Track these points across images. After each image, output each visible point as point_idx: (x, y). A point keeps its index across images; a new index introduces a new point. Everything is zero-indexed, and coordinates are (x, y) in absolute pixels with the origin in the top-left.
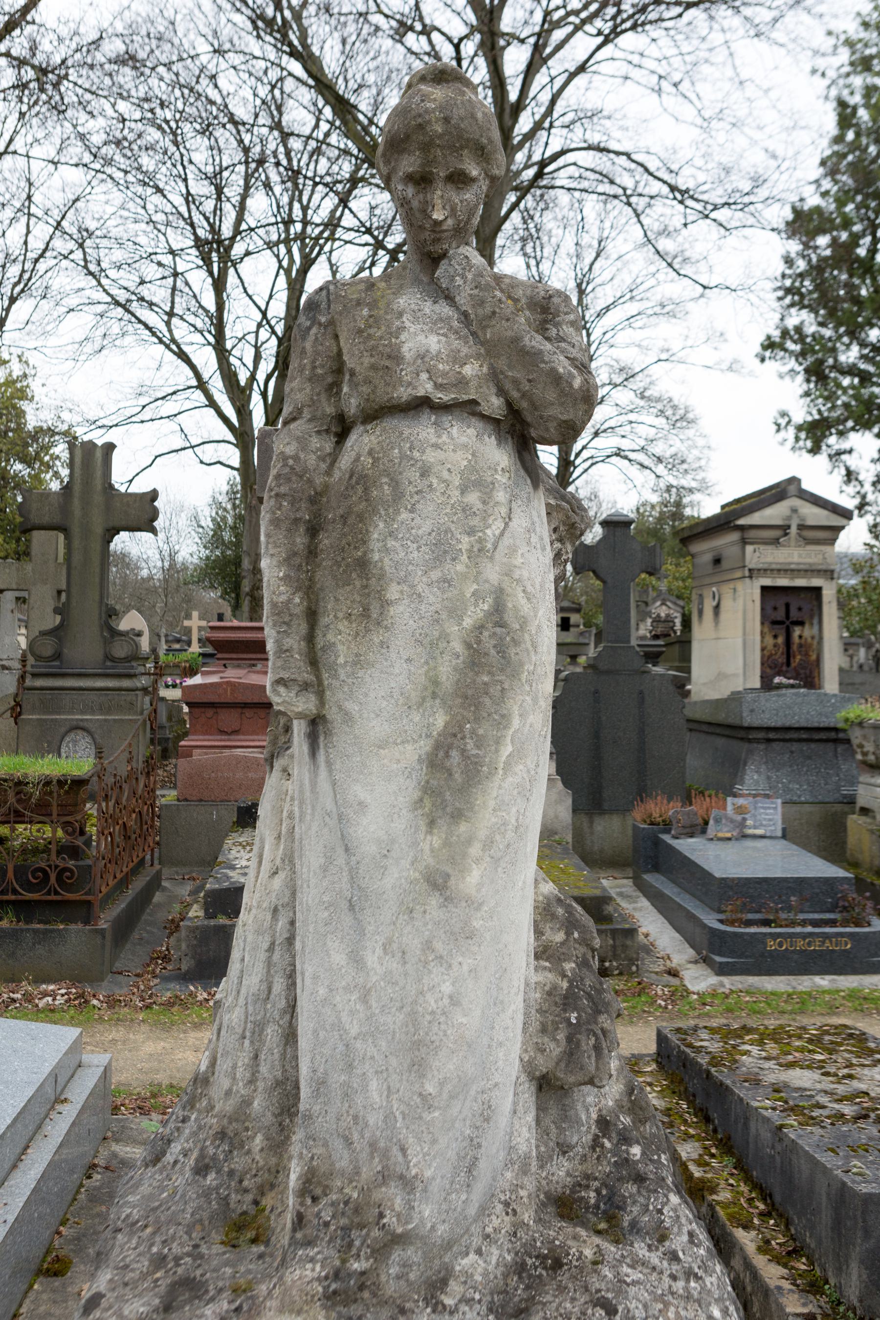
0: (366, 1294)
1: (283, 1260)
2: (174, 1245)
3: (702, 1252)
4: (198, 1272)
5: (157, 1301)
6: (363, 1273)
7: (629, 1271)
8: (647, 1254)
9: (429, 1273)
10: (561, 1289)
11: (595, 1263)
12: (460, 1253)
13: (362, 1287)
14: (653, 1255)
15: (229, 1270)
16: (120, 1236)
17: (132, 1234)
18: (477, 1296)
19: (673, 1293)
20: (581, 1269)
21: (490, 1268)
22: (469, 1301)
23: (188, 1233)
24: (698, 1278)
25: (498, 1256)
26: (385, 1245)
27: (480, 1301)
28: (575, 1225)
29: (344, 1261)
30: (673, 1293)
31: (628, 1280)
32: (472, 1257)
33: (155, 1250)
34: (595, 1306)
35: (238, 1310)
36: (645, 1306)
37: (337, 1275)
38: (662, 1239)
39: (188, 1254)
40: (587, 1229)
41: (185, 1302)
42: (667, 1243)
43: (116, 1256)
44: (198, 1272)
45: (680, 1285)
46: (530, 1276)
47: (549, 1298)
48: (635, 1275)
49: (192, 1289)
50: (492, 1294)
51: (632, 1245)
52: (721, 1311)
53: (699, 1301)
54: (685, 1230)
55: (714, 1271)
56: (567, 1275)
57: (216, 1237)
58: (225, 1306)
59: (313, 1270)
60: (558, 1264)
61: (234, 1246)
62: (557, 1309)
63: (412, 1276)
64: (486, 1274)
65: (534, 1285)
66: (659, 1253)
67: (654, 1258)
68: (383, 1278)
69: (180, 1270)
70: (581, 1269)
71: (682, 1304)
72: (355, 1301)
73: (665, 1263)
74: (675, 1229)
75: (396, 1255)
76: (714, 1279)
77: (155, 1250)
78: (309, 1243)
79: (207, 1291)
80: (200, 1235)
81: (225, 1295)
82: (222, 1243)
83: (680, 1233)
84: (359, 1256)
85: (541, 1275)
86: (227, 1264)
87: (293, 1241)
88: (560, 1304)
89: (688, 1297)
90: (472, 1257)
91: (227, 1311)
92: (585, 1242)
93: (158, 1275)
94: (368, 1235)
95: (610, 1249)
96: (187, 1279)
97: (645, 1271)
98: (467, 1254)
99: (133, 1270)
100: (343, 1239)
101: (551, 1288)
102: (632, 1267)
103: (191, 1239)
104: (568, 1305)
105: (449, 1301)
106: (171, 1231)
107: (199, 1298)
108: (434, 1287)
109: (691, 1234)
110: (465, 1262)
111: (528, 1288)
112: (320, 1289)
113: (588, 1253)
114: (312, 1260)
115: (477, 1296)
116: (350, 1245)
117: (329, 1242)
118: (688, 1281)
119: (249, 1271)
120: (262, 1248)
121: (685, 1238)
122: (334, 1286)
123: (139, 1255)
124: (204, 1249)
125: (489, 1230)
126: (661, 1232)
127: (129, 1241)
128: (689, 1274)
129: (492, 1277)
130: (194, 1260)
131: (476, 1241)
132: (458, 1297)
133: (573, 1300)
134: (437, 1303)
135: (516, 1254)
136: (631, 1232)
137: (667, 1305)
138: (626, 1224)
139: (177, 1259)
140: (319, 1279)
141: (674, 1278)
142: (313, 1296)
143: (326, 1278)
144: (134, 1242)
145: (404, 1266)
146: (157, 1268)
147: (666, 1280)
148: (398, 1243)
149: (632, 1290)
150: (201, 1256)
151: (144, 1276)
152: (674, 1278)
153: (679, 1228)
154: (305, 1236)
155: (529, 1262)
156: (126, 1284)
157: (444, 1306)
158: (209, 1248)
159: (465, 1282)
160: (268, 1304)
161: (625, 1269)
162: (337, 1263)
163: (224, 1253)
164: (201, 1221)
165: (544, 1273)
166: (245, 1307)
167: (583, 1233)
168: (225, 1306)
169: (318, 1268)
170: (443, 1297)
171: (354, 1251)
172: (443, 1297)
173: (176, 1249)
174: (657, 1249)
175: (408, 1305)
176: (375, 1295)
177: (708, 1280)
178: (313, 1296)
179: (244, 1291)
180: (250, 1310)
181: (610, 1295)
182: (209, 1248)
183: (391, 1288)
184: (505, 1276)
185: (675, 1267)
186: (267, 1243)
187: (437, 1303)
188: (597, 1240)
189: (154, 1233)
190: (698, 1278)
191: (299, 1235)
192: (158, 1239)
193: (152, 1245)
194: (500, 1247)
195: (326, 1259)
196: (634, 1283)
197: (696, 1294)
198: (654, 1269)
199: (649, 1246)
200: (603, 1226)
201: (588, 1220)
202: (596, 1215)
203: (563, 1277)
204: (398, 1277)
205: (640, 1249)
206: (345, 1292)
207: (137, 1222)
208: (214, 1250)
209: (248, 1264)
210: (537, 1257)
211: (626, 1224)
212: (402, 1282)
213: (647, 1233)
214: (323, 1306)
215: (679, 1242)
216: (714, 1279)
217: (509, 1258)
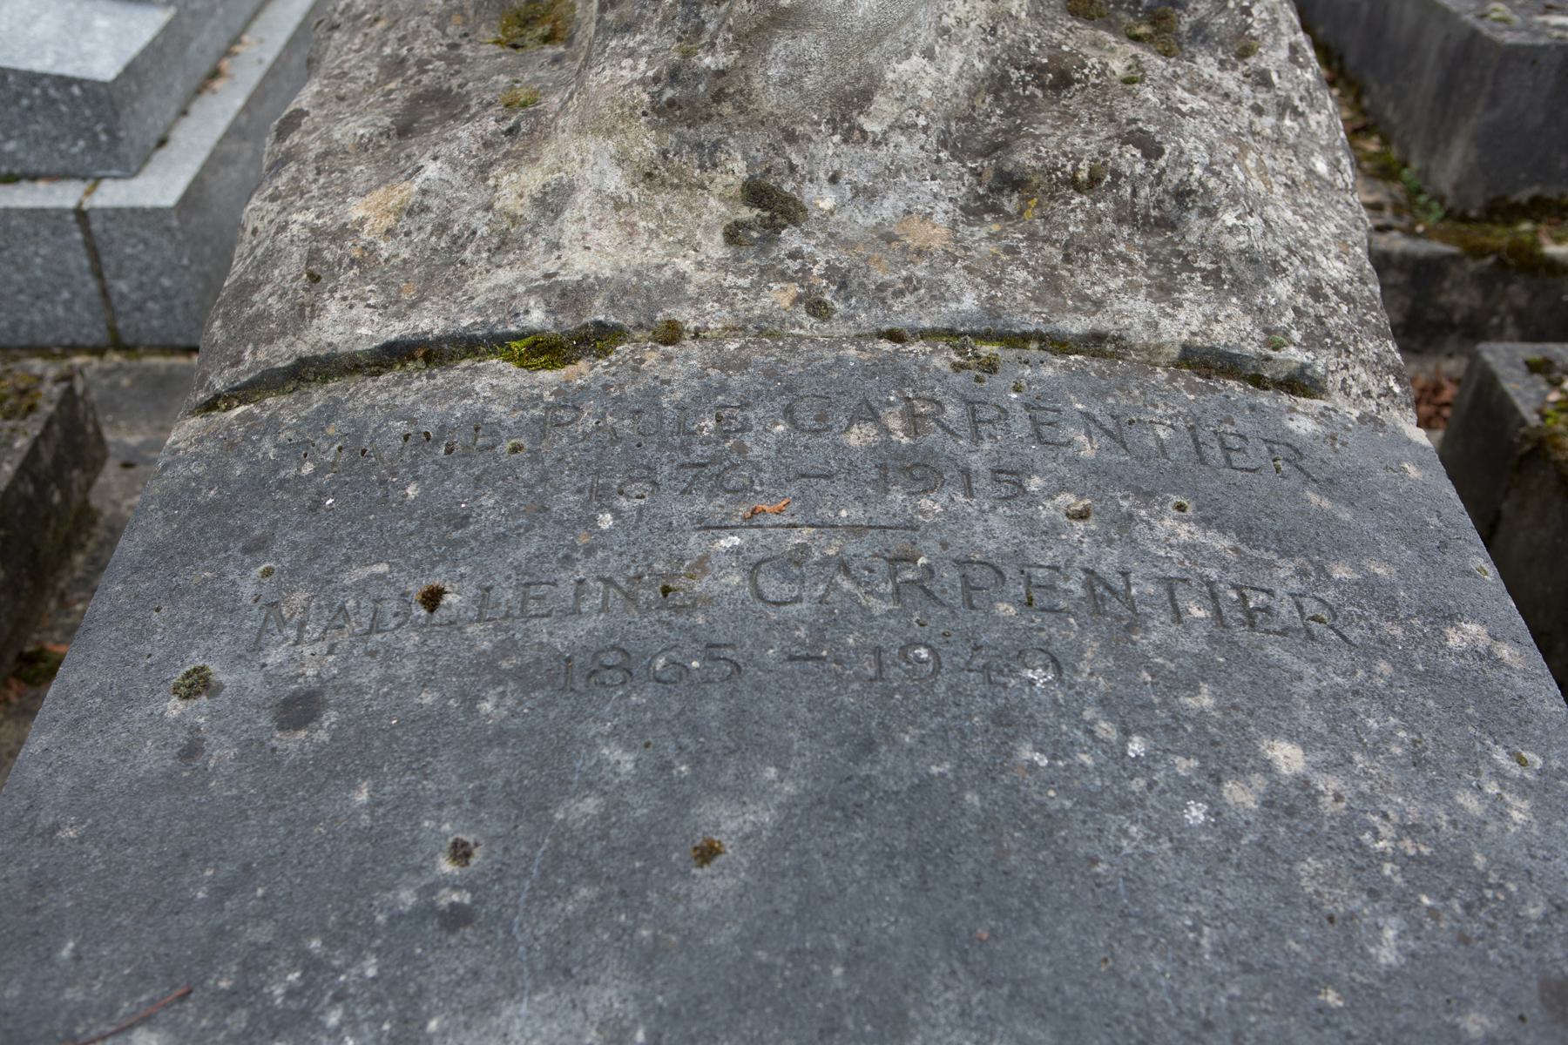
0: (727, 108)
1: (587, 59)
2: (417, 44)
3: (1309, 76)
4: (455, 82)
5: (387, 121)
6: (720, 73)
7: (1186, 95)
8: (1217, 74)
9: (840, 79)
10: (1067, 117)
11: (1128, 81)
12: (896, 53)
13: (719, 96)
14: (1226, 75)
15: (504, 79)
16: (337, 35)
17: (354, 30)
18: (922, 121)
19: (1254, 134)
20: (1103, 90)
21: (947, 80)
22: (907, 128)
23: (441, 27)
24: (1297, 114)
25: (959, 64)
26: (760, 27)
27: (925, 129)
28: (1097, 27)
29: (687, 55)
30: (1254, 134)
31: (1184, 108)
32: (917, 60)
33: (387, 51)
34: (1125, 143)
35: (510, 132)
36: (1211, 148)
37: (674, 76)
38: (1245, 53)
39: (440, 57)
40: (1115, 33)
41: (434, 123)
42: (1252, 60)
43: (329, 62)
44: (455, 82)
45: (1266, 123)
46: (1014, 97)
47: (1044, 129)
48: (1195, 103)
49: (445, 106)
50: (947, 120)
51: (1192, 59)
52: (1329, 164)
53: (1295, 148)
54: (1285, 41)
55: (1325, 107)
56: (1078, 98)
57: (487, 33)
58: (492, 125)
59: (634, 69)
60: (1063, 81)
61: (515, 47)
62: (1058, 146)
63: (809, 83)
64: (938, 88)
65: (1020, 111)
66: (1237, 74)
67: (1229, 81)
68: (757, 83)
69: (425, 79)
70: (1103, 90)
71: (1268, 150)
72: (709, 118)
73: (1246, 89)
74: (1269, 40)
75: (782, 46)
76: (1323, 118)
77: (387, 51)
78: (627, 28)
79: (468, 107)
80: (461, 30)
81: (491, 110)
82: (497, 42)
83: (1275, 45)
84: (713, 45)
85: (1033, 96)
86: (501, 70)
87: (604, 29)
88: (1064, 139)
89: (1279, 141)
90: (917, 60)
91: (494, 134)
92: (1112, 50)
93: (392, 86)
94: (729, 11)
95: (1155, 63)
96: (439, 91)
97: (1211, 98)
98: (908, 55)
99: (354, 80)
100: (686, 21)
101: (1049, 115)
102: (1191, 91)
103: (445, 35)
104: (1078, 141)
105: (871, 126)
106: (413, 23)
107: (454, 117)
108: (848, 104)
109: (1294, 49)
110: (904, 67)
111: (1009, 113)
112: (646, 97)
113: (1118, 66)
114: (632, 53)
115: (922, 121)
116: (699, 29)
117: (662, 25)
118: (1281, 117)
119: (537, 79)
120: (561, 49)
121: (1284, 54)
122: (669, 93)
123: (365, 59)
124: (466, 50)
125: (948, 21)
126: (1243, 42)
127: (350, 40)
128: (1285, 107)
129: (949, 93)
130: (449, 65)
131: (926, 36)
132: (889, 121)
133: (1087, 133)
134: (851, 129)
135: (994, 61)
136: (1192, 40)
137: (1244, 149)
138: (1184, 28)
139: (422, 65)
140: (642, 82)
141: (1258, 111)
142: (634, 108)
143: (656, 79)
144: (358, 41)
145: (795, 65)
146: (391, 76)
147: (1246, 114)
148: (782, 25)
149: (1190, 124)
150: (461, 60)
151: (370, 87)
152: (1258, 111)
153: (1276, 39)
154: (620, 16)
155: (1015, 75)
156: (342, 99)
157: (864, 133)
158: (476, 49)
159: (903, 99)
160: (561, 122)
161: (1179, 93)
162: (676, 57)
163: (499, 56)
164: (460, 10)
165: (1039, 93)
166: (524, 128)
167: (1110, 38)
168: (492, 125)
169: (642, 65)
170: (862, 119)
171: (706, 38)
172: (862, 119)
173: (420, 49)
174: (1234, 67)
175: (800, 129)
176: (742, 110)
177: (1313, 119)
178: (634, 108)
179: (524, 105)
180: (532, 131)
181: (1152, 128)
182: (476, 49)
183: (770, 100)
184: (972, 94)
185: (1262, 96)
186: (569, 42)
187: (851, 129)
188: (1134, 49)
189: (388, 29)
190: (1297, 114)
191: (610, 16)
192: (392, 35)
193: (384, 44)
194: (967, 49)
195: (655, 51)
196: (1193, 113)
197: (1292, 139)
198: (1227, 96)
199: (1222, 63)
200: (1143, 30)
201: (1119, 21)
202: (1133, 13)
203: (1072, 100)
204: (784, 83)
205: (1206, 65)
206: (690, 103)
207: (364, 13)
208: (484, 51)
209: (536, 69)
210: (1028, 68)
211: (1184, 28)
212: (791, 92)
213: (1221, 43)
214: (653, 125)
215: (1272, 58)
216: (1323, 118)
217: (980, 66)
